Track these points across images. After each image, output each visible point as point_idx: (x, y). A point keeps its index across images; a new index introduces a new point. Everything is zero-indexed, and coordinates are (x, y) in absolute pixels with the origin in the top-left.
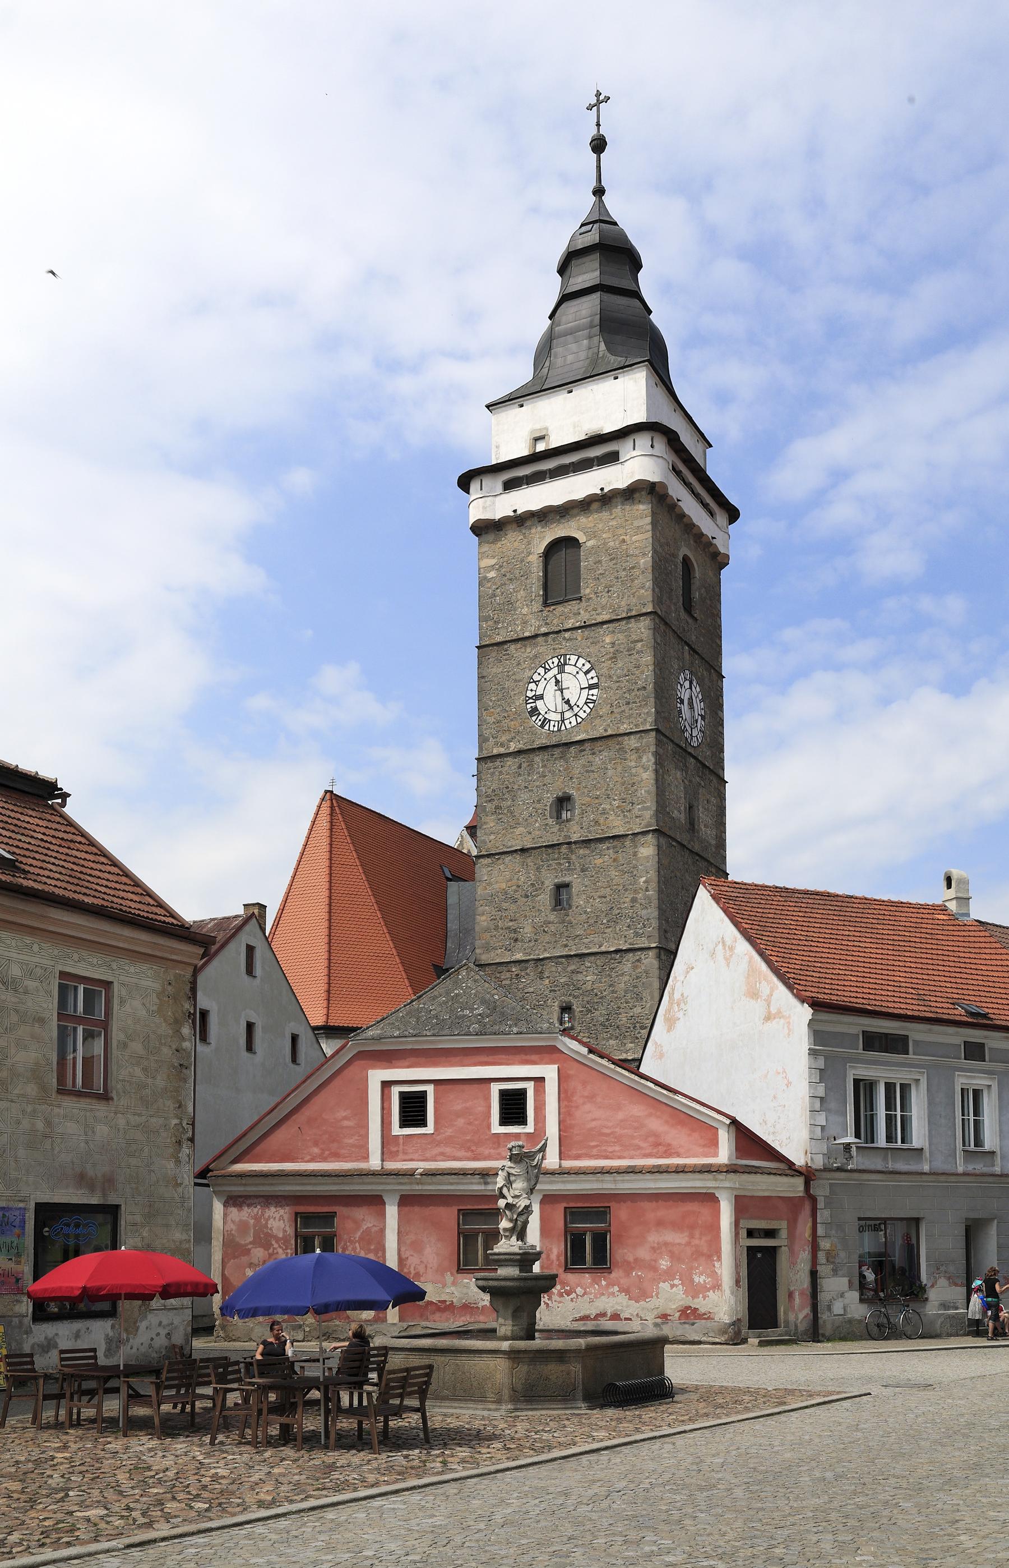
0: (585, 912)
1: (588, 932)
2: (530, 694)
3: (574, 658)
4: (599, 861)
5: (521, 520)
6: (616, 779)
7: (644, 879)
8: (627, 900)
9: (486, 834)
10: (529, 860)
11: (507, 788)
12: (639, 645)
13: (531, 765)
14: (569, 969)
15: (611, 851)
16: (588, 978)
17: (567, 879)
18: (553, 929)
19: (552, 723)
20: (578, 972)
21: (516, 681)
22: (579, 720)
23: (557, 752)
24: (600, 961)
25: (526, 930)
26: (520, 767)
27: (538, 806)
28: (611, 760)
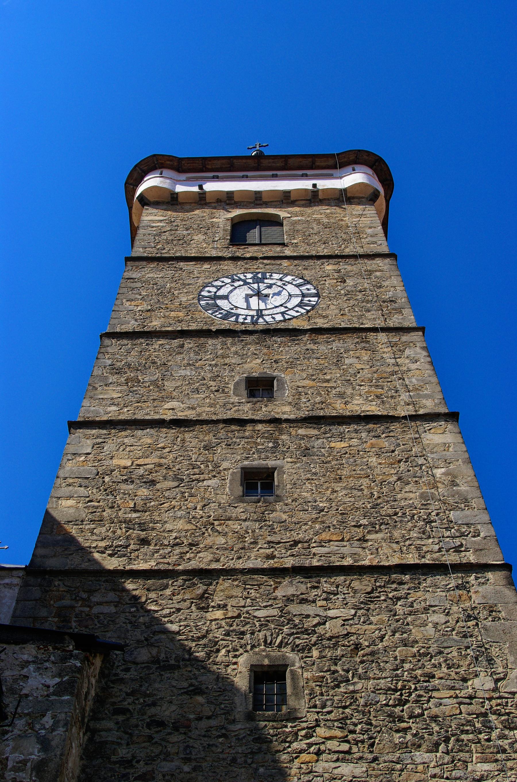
0: (315, 508)
1: (325, 536)
2: (204, 293)
3: (276, 276)
4: (339, 445)
5: (202, 200)
6: (359, 366)
7: (443, 470)
8: (412, 495)
9: (100, 404)
10: (187, 436)
11: (154, 363)
12: (378, 274)
13: (202, 346)
14: (279, 593)
15: (364, 435)
16: (331, 613)
17: (271, 463)
18: (236, 527)
19: (241, 317)
20: (304, 601)
21: (184, 284)
22: (287, 317)
23: (250, 339)
24: (363, 584)
25: (168, 527)
26: (182, 346)
27: (212, 383)
28: (347, 351)
